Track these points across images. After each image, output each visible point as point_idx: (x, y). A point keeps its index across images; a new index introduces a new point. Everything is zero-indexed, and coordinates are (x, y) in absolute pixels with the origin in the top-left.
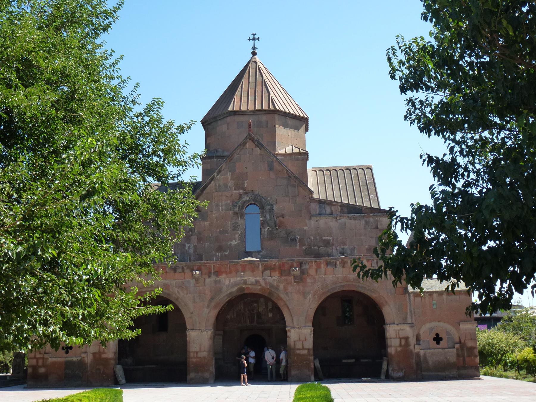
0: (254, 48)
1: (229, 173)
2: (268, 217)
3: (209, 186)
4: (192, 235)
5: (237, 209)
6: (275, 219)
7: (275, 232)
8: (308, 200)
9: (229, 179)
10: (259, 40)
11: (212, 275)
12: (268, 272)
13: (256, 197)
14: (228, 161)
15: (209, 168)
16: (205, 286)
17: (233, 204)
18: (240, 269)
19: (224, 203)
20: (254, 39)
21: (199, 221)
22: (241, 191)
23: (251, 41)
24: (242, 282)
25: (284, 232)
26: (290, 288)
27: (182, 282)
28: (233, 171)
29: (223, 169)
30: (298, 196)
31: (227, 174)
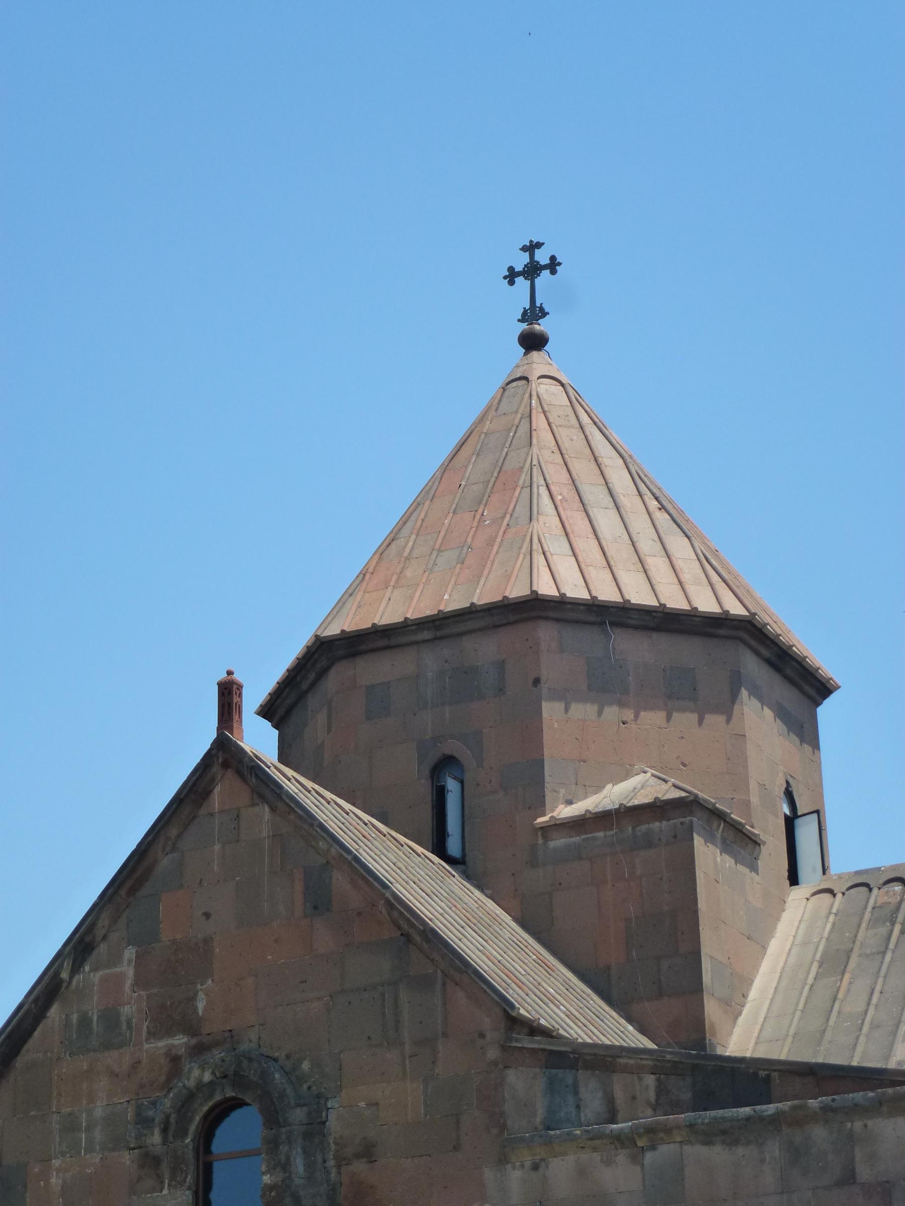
0: (534, 313)
1: (130, 953)
2: (299, 1165)
3: (36, 1034)
8: (493, 1054)
9: (128, 983)
10: (553, 272)
13: (245, 1063)
14: (123, 892)
17: (138, 1114)
19: (99, 1112)
20: (532, 271)
22: (180, 1041)
23: (520, 280)
29: (100, 932)
30: (445, 1035)
31: (115, 959)
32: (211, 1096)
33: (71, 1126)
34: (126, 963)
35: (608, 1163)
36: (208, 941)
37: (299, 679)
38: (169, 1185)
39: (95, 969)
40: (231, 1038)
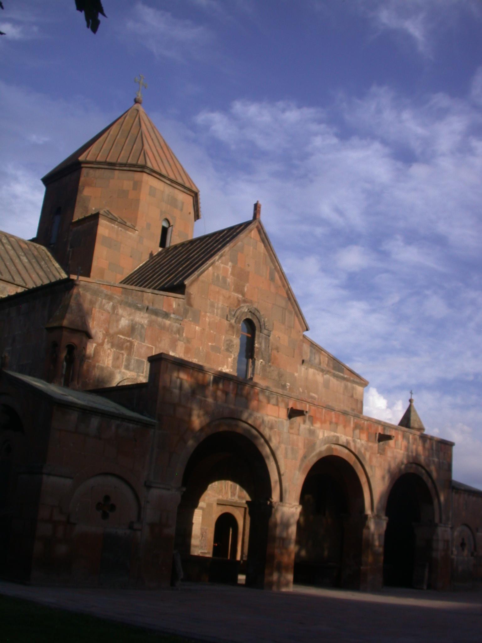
1: (230, 264)
3: (206, 272)
4: (179, 340)
5: (233, 321)
6: (270, 351)
7: (268, 369)
9: (229, 273)
11: (307, 421)
12: (357, 432)
15: (107, 235)
16: (298, 434)
17: (230, 311)
18: (334, 420)
19: (220, 305)
21: (190, 321)
22: (240, 296)
24: (335, 439)
25: (276, 373)
26: (374, 460)
27: (276, 421)
28: (234, 261)
31: (227, 264)
32: (246, 316)
33: (212, 306)
34: (229, 266)
35: (318, 374)
36: (248, 272)
37: (117, 165)
38: (236, 336)
39: (222, 263)
40: (251, 302)
